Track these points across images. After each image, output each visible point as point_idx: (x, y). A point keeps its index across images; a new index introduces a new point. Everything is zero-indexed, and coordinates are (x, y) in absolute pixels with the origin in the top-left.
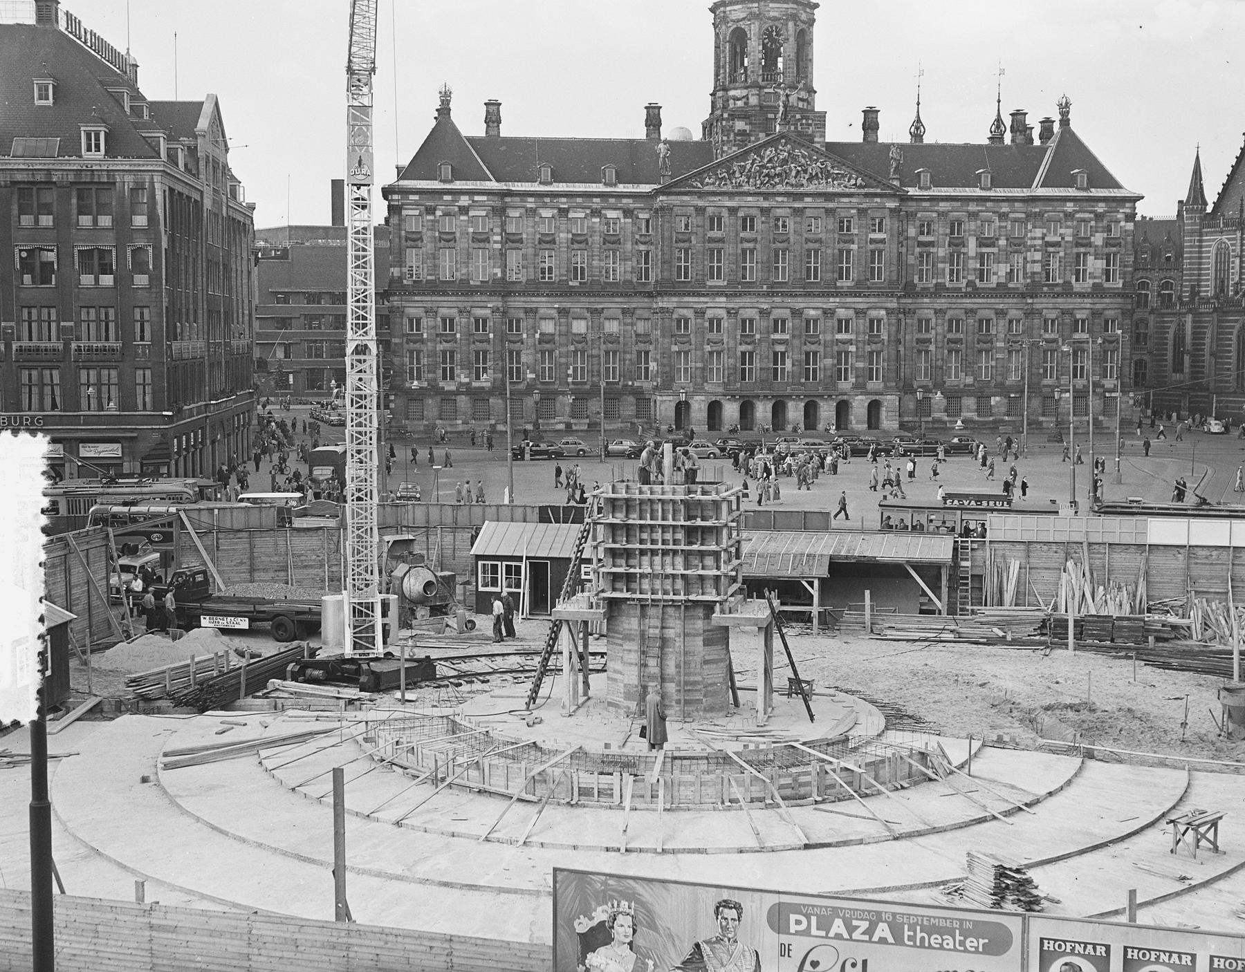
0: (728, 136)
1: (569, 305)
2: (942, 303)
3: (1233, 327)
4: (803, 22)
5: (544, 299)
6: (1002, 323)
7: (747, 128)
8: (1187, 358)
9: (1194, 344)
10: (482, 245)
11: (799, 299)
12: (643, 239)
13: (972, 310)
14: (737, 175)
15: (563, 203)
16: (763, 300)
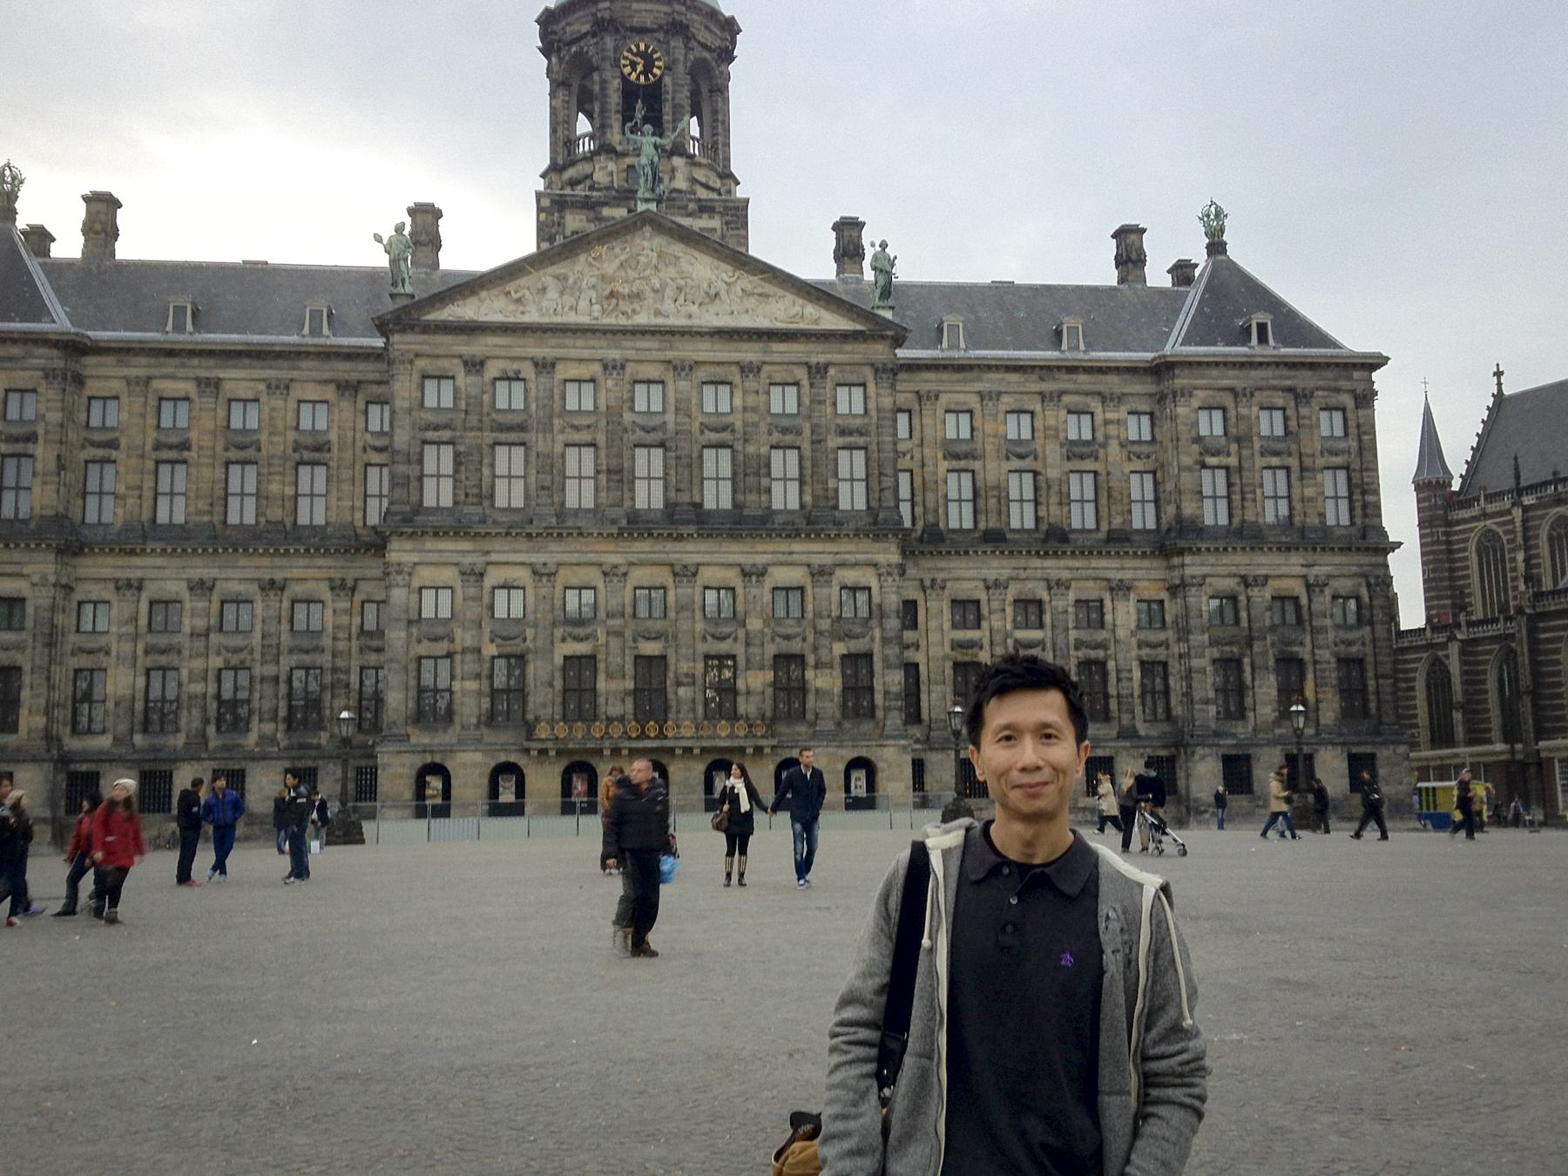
0: (551, 239)
1: (214, 573)
2: (997, 568)
3: (1559, 639)
4: (704, 46)
5: (159, 561)
6: (1120, 606)
7: (591, 227)
8: (1457, 716)
9: (1465, 693)
10: (19, 447)
11: (690, 546)
12: (380, 443)
13: (1059, 583)
14: (552, 294)
15: (207, 369)
16: (612, 548)
